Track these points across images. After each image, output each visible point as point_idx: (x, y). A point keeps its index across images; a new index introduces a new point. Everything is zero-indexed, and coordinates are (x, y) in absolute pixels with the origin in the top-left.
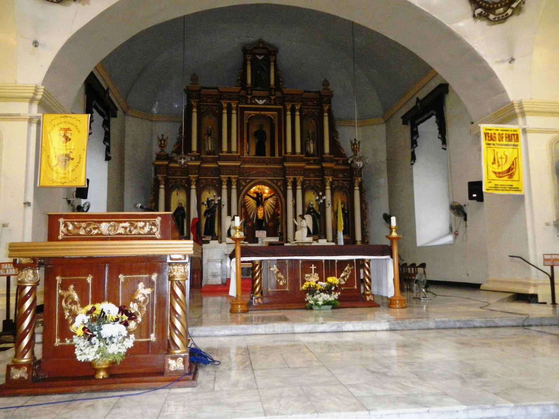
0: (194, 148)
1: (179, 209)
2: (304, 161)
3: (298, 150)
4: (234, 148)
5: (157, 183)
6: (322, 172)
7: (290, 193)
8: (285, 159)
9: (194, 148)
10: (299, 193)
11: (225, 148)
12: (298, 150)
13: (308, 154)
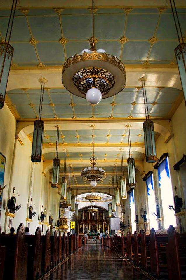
0: (83, 219)
1: (81, 228)
2: (100, 220)
3: (99, 218)
4: (89, 218)
5: (78, 224)
6: (102, 222)
7: (98, 226)
8: (97, 220)
9: (83, 219)
10: (99, 225)
11: (88, 218)
12: (99, 218)
13: (101, 219)
